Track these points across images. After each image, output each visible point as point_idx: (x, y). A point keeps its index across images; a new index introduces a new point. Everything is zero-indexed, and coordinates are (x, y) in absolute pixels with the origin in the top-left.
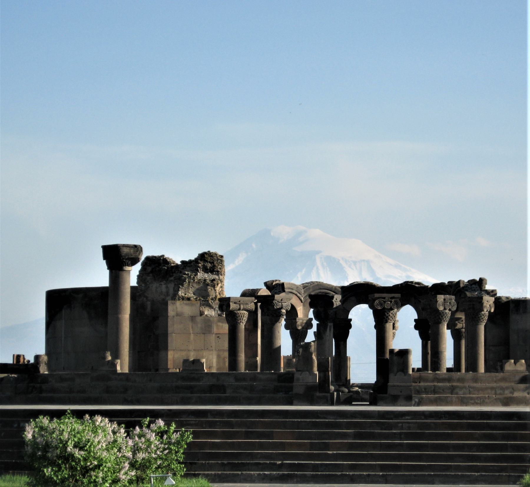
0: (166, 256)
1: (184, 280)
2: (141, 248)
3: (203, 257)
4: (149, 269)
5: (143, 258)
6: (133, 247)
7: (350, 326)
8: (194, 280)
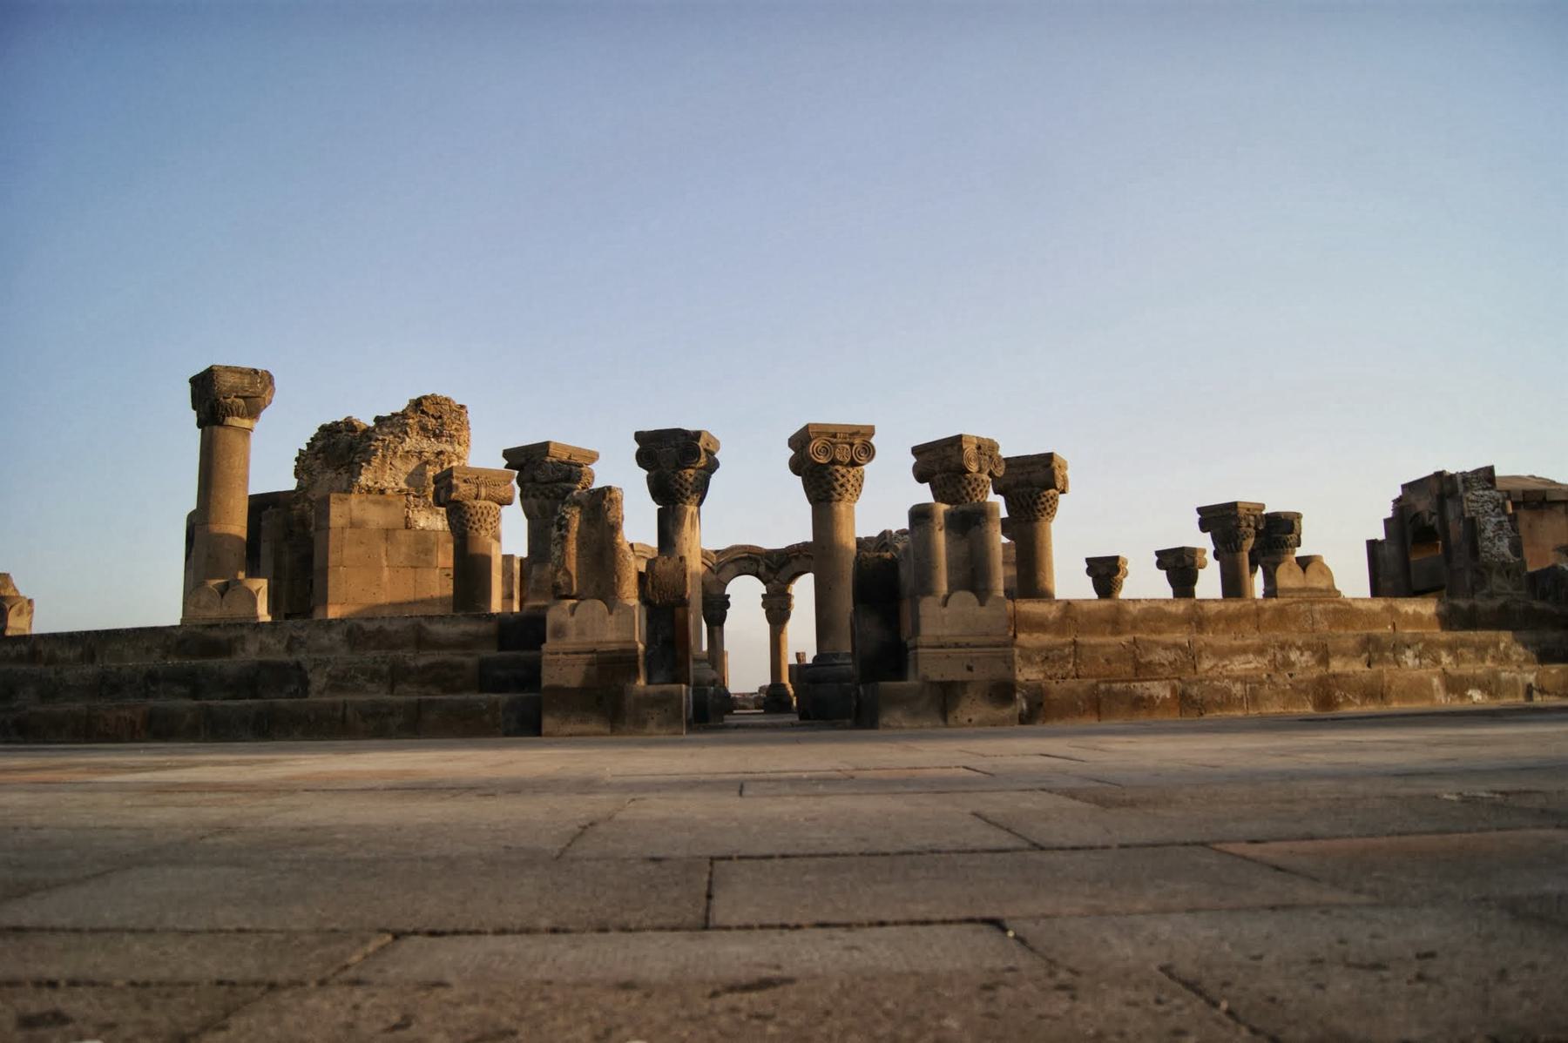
2: (270, 377)
3: (417, 404)
4: (319, 444)
6: (250, 374)
7: (728, 605)
8: (395, 453)
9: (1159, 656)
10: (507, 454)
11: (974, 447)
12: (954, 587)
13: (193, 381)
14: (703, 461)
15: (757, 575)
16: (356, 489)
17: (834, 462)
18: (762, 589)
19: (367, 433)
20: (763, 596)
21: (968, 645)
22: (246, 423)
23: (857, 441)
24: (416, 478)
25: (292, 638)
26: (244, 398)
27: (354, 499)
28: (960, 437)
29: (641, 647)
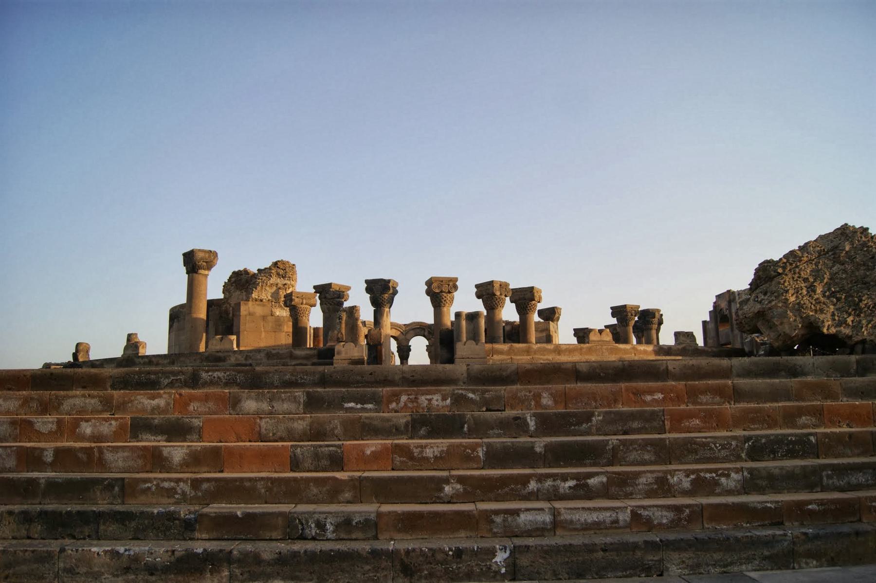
1: (258, 284)
2: (217, 254)
3: (276, 264)
4: (233, 280)
7: (410, 350)
8: (267, 284)
10: (315, 287)
11: (498, 285)
12: (467, 339)
13: (185, 255)
14: (391, 291)
15: (424, 336)
16: (251, 299)
17: (442, 292)
18: (427, 343)
19: (254, 276)
20: (427, 346)
21: (472, 358)
22: (206, 272)
23: (451, 284)
24: (275, 295)
25: (247, 356)
26: (206, 262)
27: (250, 303)
28: (493, 281)
29: (366, 358)
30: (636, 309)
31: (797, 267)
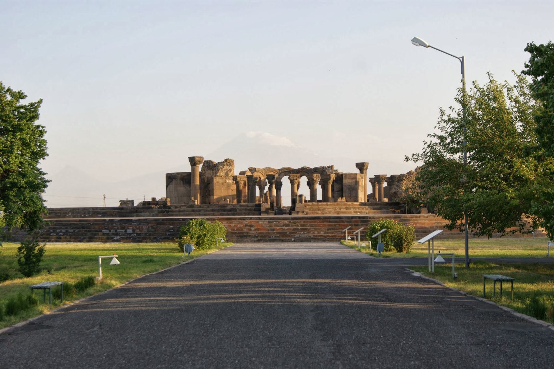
0: (212, 160)
1: (219, 170)
3: (226, 160)
4: (206, 165)
5: (203, 161)
7: (282, 184)
9: (321, 209)
24: (227, 174)
27: (217, 178)
30: (385, 177)
31: (411, 177)
